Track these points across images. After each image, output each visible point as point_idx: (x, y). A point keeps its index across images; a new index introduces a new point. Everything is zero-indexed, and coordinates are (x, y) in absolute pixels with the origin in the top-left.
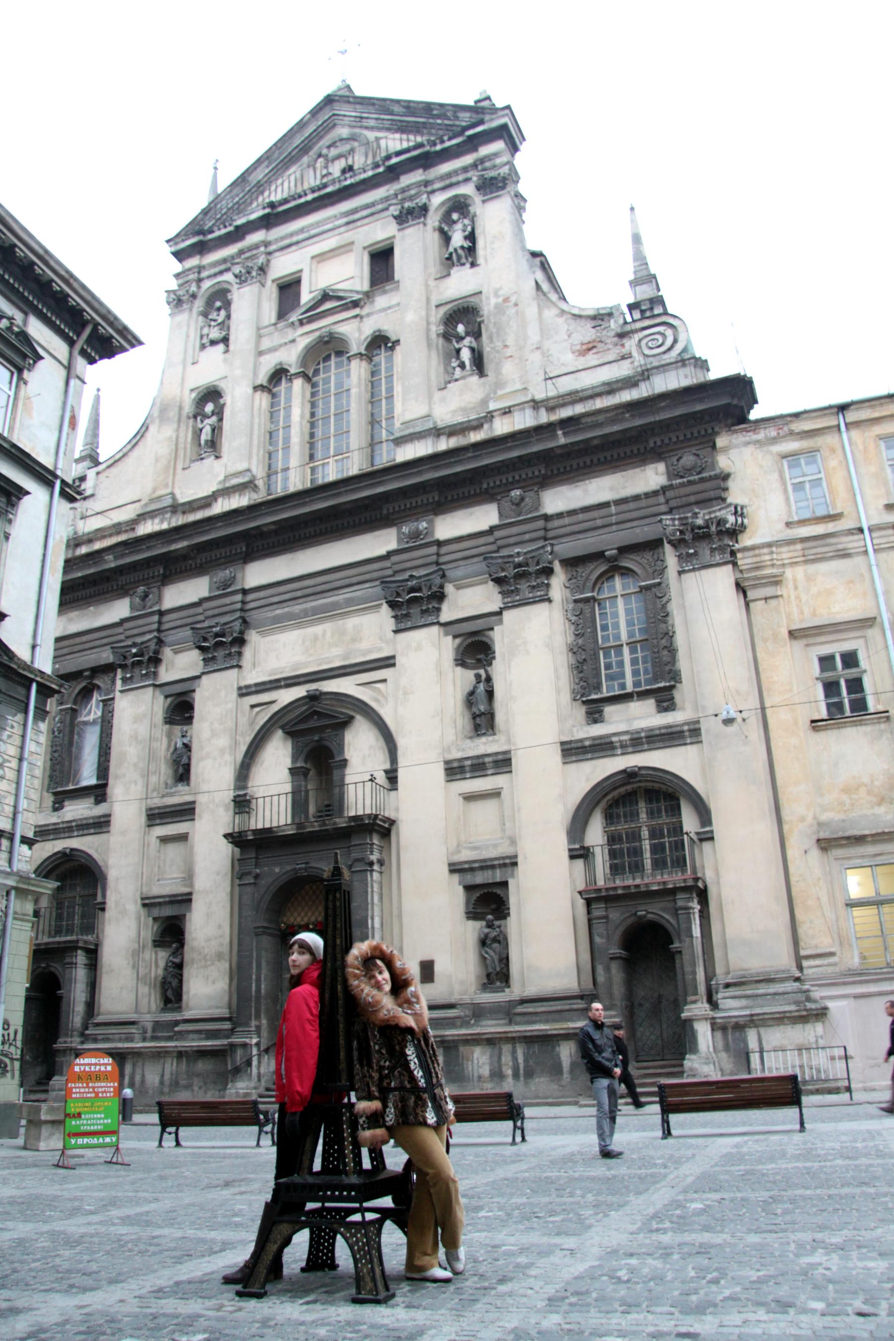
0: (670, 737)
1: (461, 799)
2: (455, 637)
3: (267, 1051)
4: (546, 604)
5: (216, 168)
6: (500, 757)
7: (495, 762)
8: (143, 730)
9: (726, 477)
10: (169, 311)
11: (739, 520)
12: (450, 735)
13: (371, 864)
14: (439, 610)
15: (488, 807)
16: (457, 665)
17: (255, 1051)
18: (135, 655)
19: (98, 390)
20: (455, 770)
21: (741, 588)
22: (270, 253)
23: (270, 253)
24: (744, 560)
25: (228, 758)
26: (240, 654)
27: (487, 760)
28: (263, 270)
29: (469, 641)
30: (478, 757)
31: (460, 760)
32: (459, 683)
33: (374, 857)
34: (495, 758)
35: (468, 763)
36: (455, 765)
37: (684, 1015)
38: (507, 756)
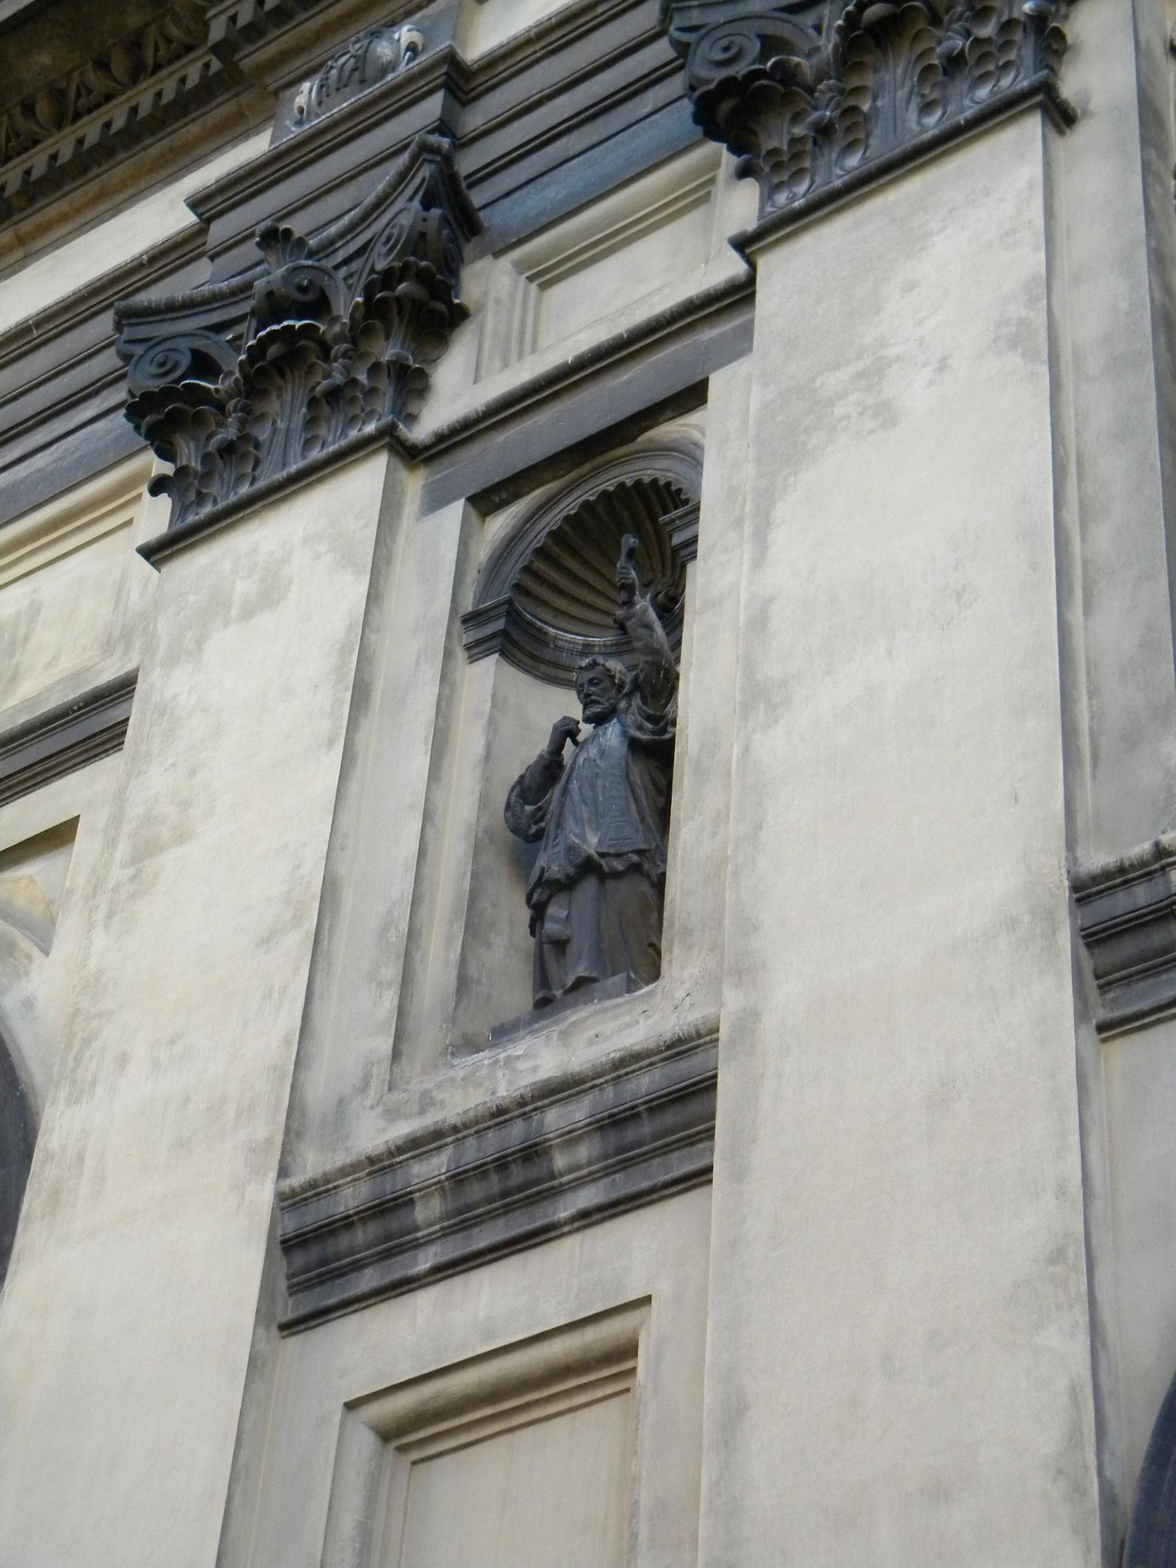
1: (363, 1441)
2: (486, 501)
4: (1032, 126)
6: (645, 1083)
7: (612, 1122)
14: (412, 383)
15: (551, 1467)
16: (476, 650)
27: (555, 1119)
29: (570, 506)
30: (500, 1115)
31: (379, 1165)
32: (469, 741)
34: (609, 1098)
35: (438, 1165)
36: (351, 1198)
38: (688, 1069)
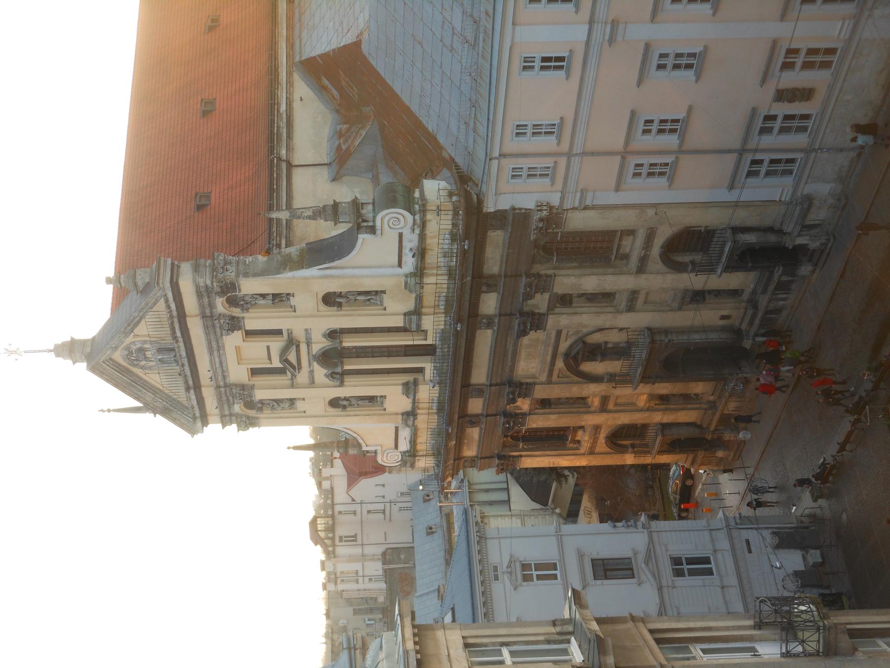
0: (651, 235)
3: (740, 369)
5: (109, 411)
8: (553, 417)
9: (514, 209)
10: (256, 429)
11: (545, 208)
12: (611, 309)
13: (669, 341)
17: (740, 375)
18: (509, 424)
19: (289, 448)
20: (630, 308)
21: (586, 208)
22: (225, 383)
23: (225, 383)
24: (568, 205)
25: (585, 386)
26: (527, 384)
28: (243, 387)
33: (667, 340)
37: (790, 248)
